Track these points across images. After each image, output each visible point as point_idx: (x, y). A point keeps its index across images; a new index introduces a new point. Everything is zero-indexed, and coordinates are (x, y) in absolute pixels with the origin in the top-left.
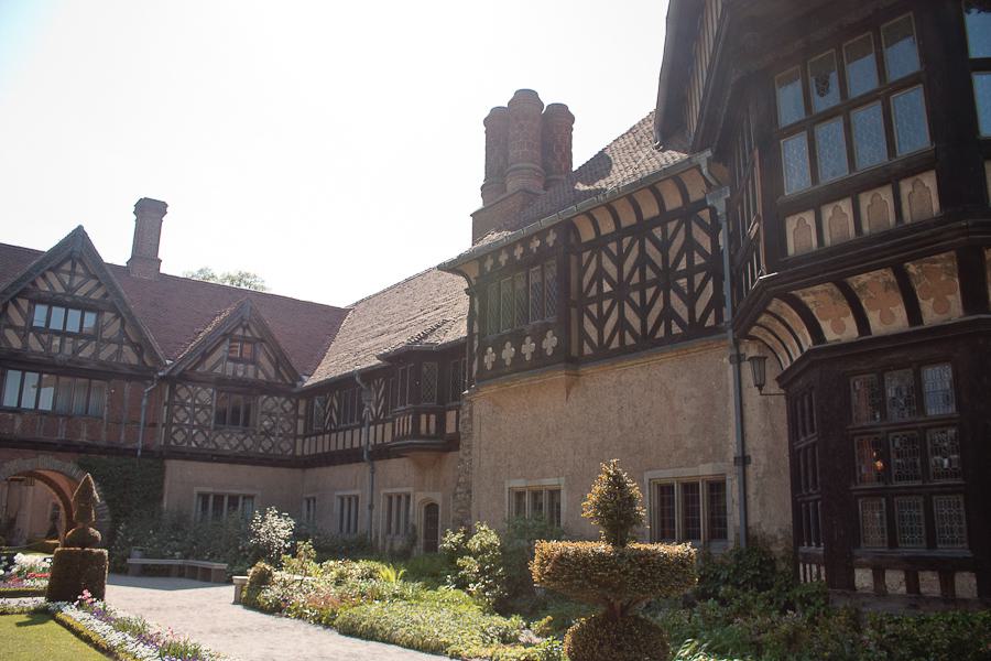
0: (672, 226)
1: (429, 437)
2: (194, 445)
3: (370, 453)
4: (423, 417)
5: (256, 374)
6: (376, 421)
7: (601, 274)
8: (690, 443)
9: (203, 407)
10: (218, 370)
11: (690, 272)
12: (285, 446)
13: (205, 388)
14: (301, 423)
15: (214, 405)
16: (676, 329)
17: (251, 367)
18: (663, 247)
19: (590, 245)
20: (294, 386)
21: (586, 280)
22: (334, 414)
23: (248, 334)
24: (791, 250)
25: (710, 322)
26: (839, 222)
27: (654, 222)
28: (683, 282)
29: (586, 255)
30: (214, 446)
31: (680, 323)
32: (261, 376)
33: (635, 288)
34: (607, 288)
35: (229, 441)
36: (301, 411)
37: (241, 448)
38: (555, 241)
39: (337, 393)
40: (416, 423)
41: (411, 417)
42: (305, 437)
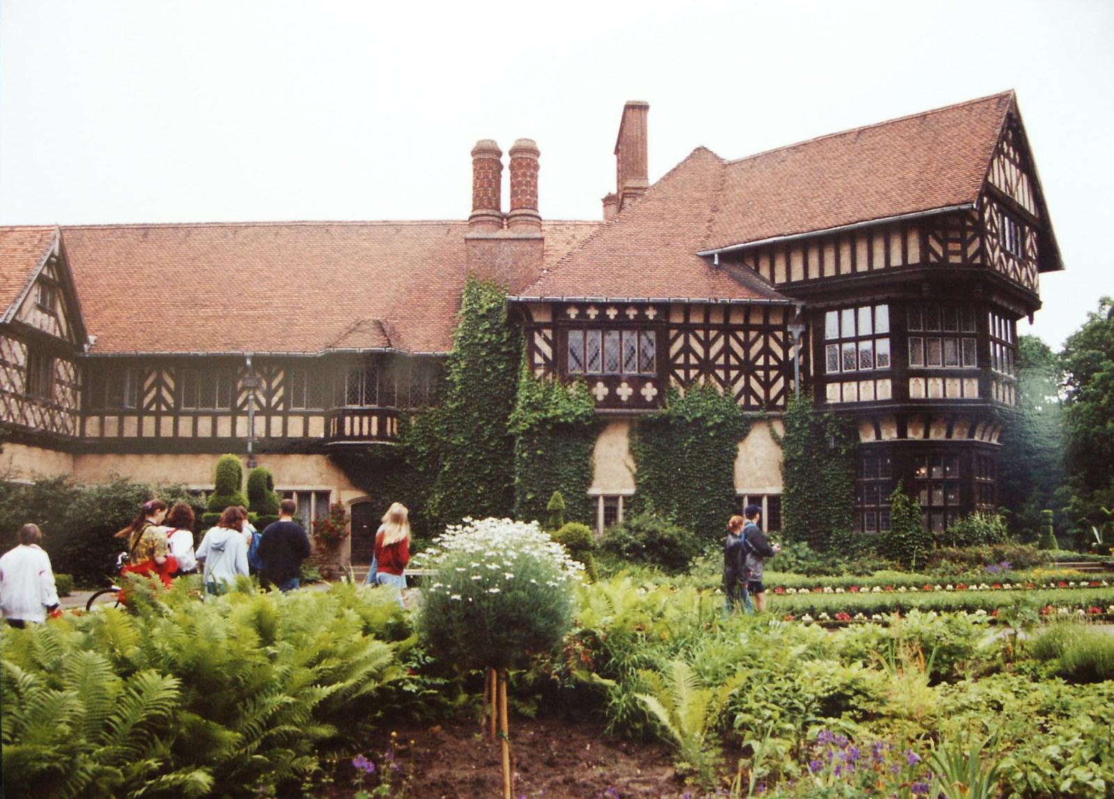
0: (753, 334)
1: (393, 439)
2: (11, 420)
3: (254, 446)
4: (389, 420)
5: (55, 331)
6: (268, 412)
7: (687, 350)
8: (759, 474)
9: (19, 369)
10: (29, 321)
11: (767, 368)
12: (69, 424)
13: (20, 344)
14: (79, 393)
15: (25, 366)
16: (753, 402)
17: (52, 319)
18: (746, 345)
19: (677, 326)
20: (82, 349)
21: (674, 349)
22: (165, 393)
23: (51, 276)
24: (912, 395)
25: (781, 402)
26: (935, 389)
27: (739, 327)
28: (760, 373)
29: (673, 333)
30: (24, 423)
31: (757, 397)
32: (58, 334)
33: (720, 367)
34: (693, 361)
35: (34, 418)
36: (79, 383)
37: (42, 427)
38: (655, 316)
39: (173, 370)
40: (382, 426)
41: (375, 419)
42: (85, 413)
